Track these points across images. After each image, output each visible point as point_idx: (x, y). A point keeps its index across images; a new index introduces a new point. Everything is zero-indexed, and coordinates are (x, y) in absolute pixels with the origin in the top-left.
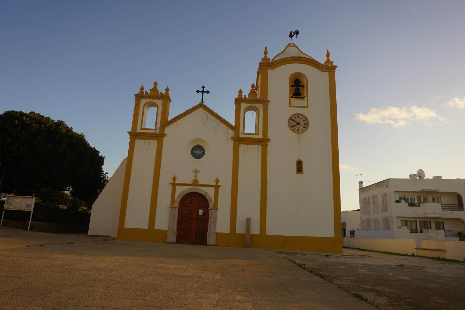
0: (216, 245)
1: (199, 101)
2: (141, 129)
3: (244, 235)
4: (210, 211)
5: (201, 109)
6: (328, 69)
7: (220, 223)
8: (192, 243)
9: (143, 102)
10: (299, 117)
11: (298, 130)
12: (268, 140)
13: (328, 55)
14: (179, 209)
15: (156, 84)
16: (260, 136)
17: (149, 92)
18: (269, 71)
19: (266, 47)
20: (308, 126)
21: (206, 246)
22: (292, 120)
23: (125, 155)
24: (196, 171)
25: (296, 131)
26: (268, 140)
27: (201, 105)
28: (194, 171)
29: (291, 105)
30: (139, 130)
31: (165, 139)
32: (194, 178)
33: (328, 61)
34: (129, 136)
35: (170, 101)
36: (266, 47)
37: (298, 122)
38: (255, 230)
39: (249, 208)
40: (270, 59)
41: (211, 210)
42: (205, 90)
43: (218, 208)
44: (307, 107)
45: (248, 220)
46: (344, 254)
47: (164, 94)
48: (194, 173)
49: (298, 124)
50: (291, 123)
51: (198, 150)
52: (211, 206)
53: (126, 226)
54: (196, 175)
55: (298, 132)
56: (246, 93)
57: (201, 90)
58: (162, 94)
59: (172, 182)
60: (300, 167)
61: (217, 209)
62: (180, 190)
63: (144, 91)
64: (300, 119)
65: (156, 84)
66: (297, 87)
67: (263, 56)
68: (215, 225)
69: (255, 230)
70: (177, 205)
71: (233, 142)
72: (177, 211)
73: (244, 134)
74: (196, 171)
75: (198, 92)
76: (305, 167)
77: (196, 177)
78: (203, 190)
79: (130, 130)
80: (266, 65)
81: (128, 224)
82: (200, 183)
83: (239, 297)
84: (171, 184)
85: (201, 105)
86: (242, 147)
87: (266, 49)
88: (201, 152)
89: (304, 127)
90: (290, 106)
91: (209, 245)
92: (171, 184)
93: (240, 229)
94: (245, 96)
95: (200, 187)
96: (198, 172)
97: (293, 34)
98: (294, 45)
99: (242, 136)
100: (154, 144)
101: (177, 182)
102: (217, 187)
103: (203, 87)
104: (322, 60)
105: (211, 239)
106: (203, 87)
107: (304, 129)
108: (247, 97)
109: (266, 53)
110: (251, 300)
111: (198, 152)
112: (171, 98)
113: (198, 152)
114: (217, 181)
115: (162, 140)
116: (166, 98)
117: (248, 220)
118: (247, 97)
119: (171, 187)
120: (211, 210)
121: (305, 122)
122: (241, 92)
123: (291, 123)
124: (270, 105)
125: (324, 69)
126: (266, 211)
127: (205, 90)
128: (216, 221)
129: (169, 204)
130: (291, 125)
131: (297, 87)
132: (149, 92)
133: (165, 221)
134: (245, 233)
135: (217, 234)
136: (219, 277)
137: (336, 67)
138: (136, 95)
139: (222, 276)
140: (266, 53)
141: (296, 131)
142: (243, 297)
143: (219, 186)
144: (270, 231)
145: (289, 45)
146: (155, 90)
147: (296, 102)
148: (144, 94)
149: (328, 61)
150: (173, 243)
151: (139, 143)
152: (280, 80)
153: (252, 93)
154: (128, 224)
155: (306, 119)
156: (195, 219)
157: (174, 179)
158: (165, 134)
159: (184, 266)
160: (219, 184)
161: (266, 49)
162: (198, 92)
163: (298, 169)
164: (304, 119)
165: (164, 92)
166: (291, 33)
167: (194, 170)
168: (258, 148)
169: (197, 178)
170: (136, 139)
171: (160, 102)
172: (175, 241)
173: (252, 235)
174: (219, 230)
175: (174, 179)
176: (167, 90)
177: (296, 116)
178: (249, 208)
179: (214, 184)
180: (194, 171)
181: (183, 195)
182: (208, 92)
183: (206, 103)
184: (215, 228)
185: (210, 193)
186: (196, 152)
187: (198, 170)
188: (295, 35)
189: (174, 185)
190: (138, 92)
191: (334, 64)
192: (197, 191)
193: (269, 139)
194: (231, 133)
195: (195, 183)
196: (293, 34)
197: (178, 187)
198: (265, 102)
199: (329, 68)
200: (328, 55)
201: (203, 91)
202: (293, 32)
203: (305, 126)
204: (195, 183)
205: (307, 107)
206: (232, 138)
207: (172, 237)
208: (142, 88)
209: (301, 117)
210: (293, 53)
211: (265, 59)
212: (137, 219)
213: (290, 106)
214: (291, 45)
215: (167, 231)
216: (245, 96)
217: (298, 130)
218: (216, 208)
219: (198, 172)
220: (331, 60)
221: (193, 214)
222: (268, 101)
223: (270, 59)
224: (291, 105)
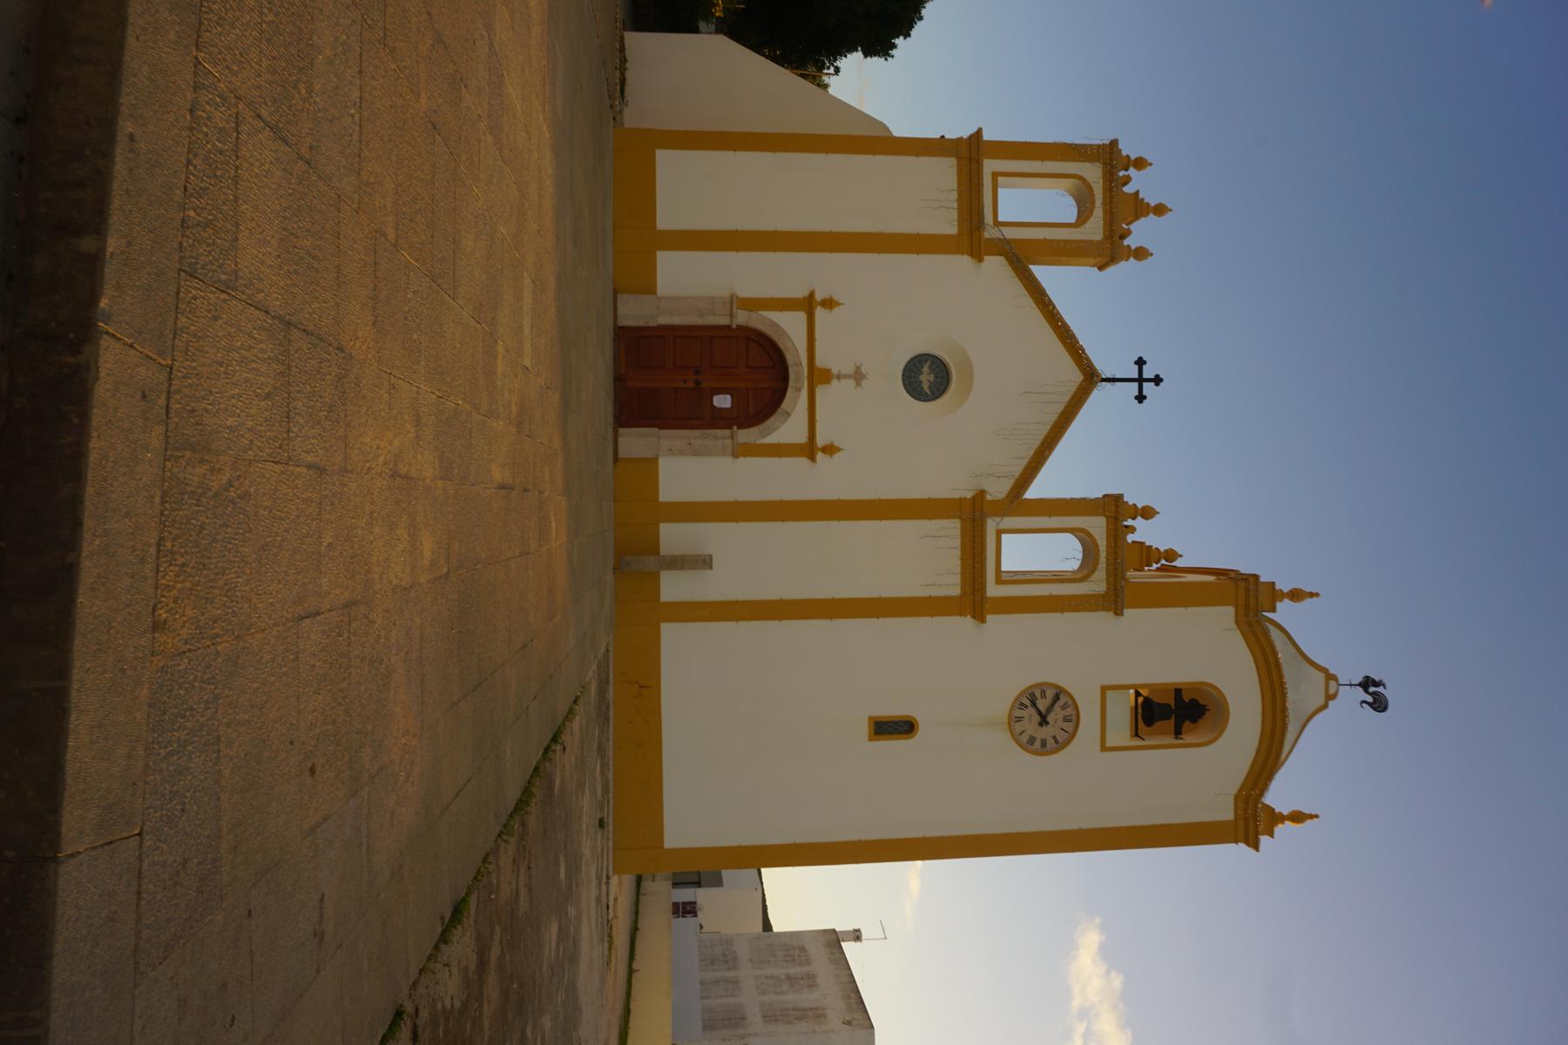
0: (616, 459)
1: (1105, 369)
2: (995, 175)
3: (655, 550)
4: (727, 432)
5: (1079, 377)
6: (1246, 819)
7: (689, 469)
8: (619, 380)
9: (1093, 172)
10: (1066, 719)
11: (1019, 719)
13: (1298, 817)
14: (729, 327)
15: (1160, 210)
16: (993, 590)
17: (1128, 189)
18: (1230, 610)
20: (1036, 753)
21: (610, 430)
22: (1057, 698)
23: (899, 131)
24: (858, 376)
25: (1018, 713)
27: (1091, 378)
28: (858, 368)
29: (1109, 694)
30: (990, 166)
31: (965, 261)
32: (835, 371)
33: (1275, 818)
34: (966, 135)
35: (1101, 268)
37: (1049, 719)
38: (674, 587)
39: (744, 561)
40: (1274, 611)
41: (732, 437)
42: (1148, 388)
43: (741, 459)
44: (1104, 748)
45: (705, 562)
46: (614, 880)
47: (1126, 242)
48: (851, 371)
49: (1044, 716)
50: (1043, 692)
52: (745, 435)
54: (847, 377)
55: (1014, 720)
56: (1143, 532)
57: (1148, 373)
58: (1123, 237)
59: (819, 297)
61: (735, 455)
62: (790, 327)
63: (1132, 171)
64: (1061, 723)
65: (1160, 210)
66: (1175, 712)
67: (1284, 586)
68: (681, 453)
69: (674, 587)
70: (742, 318)
71: (969, 495)
72: (723, 321)
73: (999, 533)
74: (858, 376)
75: (1140, 362)
77: (839, 377)
79: (987, 136)
80: (1248, 598)
81: (667, 162)
82: (820, 392)
83: (427, 545)
84: (812, 294)
85: (1091, 378)
86: (951, 529)
87: (1312, 595)
88: (926, 387)
89: (1032, 740)
90: (1104, 689)
92: (812, 294)
93: (674, 537)
94: (1132, 529)
96: (858, 384)
97: (1372, 689)
98: (1330, 697)
99: (991, 525)
100: (946, 223)
101: (819, 312)
102: (809, 450)
103: (1157, 380)
104: (1277, 797)
105: (635, 442)
106: (1157, 380)
107: (1024, 738)
108: (1130, 538)
109: (1296, 595)
110: (422, 580)
111: (928, 377)
112: (1111, 270)
113: (926, 378)
114: (830, 450)
115: (959, 252)
116: (1110, 250)
117: (705, 562)
118: (1130, 538)
119: (801, 293)
120: (732, 437)
121: (1051, 743)
122: (1148, 513)
123: (1043, 692)
124: (1104, 618)
125: (1246, 803)
126: (738, 619)
127: (1148, 388)
128: (696, 453)
129: (743, 293)
130: (1038, 695)
131: (1175, 712)
132: (1128, 189)
133: (687, 284)
134: (663, 552)
135: (655, 461)
136: (498, 475)
137: (1257, 848)
138: (1114, 143)
139: (502, 487)
140: (1296, 595)
141: (1018, 713)
142: (428, 554)
143: (812, 458)
144: (673, 636)
145: (1330, 677)
146: (1140, 208)
147: (1122, 710)
148: (1122, 173)
149: (1275, 818)
150: (615, 315)
151: (945, 172)
152: (1200, 649)
153: (1146, 554)
154: (667, 162)
155: (1060, 745)
156: (698, 383)
157: (829, 304)
158: (980, 260)
159: (524, 351)
160: (820, 456)
161: (1312, 595)
162: (1140, 362)
163: (885, 723)
164: (1061, 737)
165: (1132, 242)
166: (1377, 684)
168: (951, 585)
169: (835, 382)
170: (959, 159)
171: (1094, 230)
172: (623, 322)
173: (658, 574)
174: (665, 464)
175: (829, 304)
176: (1141, 254)
177: (1069, 711)
178: (744, 561)
179: (820, 441)
180: (858, 368)
181: (775, 338)
182: (1141, 398)
183: (1100, 393)
184: (671, 452)
185: (789, 427)
186: (926, 369)
187: (864, 383)
188: (1370, 699)
189: (808, 305)
190: (1128, 149)
191: (1264, 839)
192: (791, 383)
193: (983, 620)
194: (998, 490)
195: (819, 376)
196: (1372, 689)
197: (800, 318)
198: (1115, 600)
199: (1250, 821)
200: (1298, 817)
201: (1142, 380)
202: (1380, 689)
203: (1038, 744)
204: (819, 376)
205: (1104, 748)
206: (982, 493)
207: (634, 312)
208: (1140, 163)
209: (1069, 727)
210: (1301, 691)
211: (1273, 594)
212: (687, 189)
213: (1104, 689)
214: (1332, 683)
215: (652, 290)
216: (1132, 529)
217: (1019, 719)
218: (741, 451)
219: (858, 384)
220: (1280, 829)
221: (716, 376)
222: (1118, 612)
223: (1274, 611)
224: (1109, 694)
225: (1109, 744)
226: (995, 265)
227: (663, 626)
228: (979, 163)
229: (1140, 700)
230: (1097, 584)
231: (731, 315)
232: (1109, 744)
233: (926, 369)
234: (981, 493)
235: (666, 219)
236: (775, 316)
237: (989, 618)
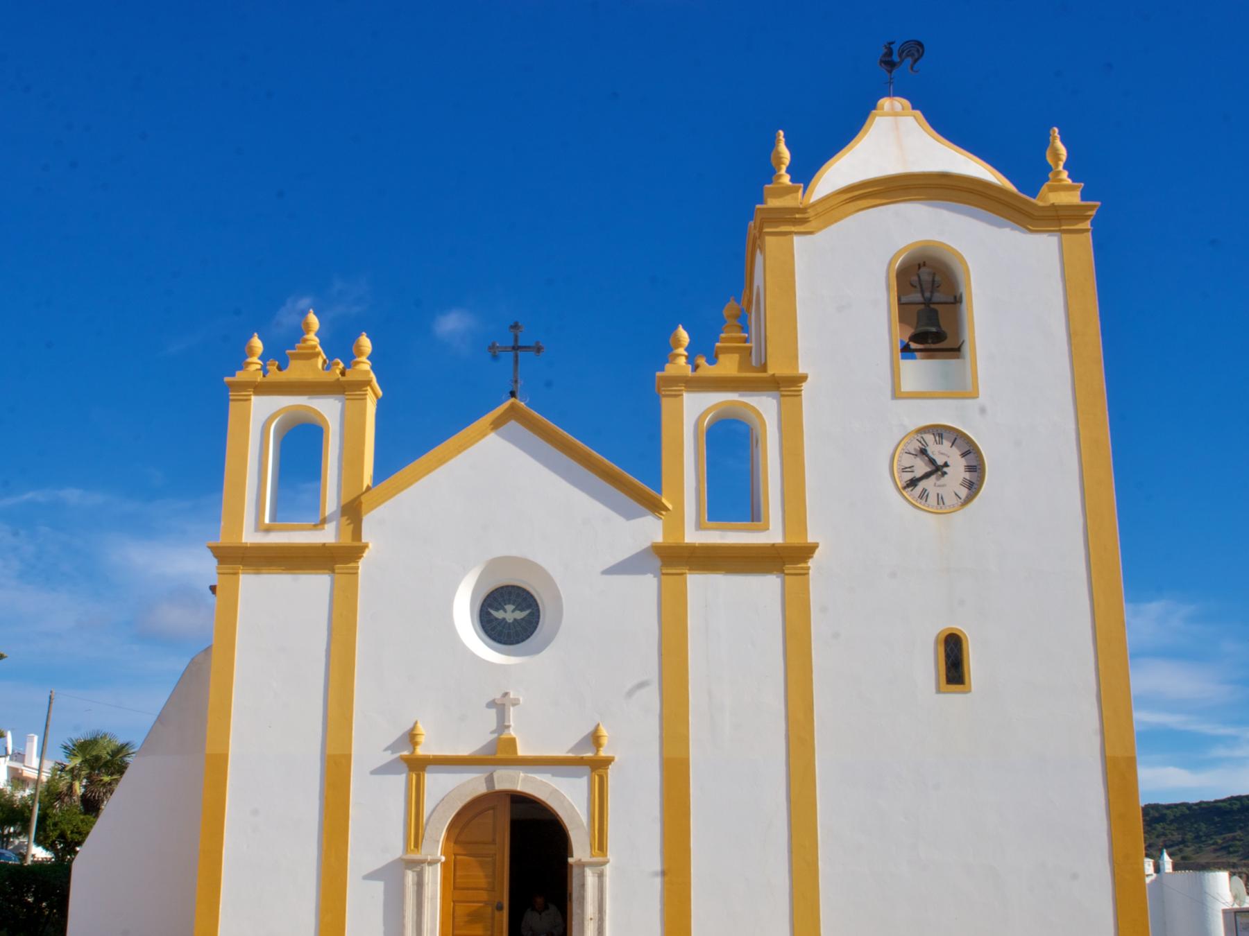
11: (940, 499)
12: (805, 552)
16: (772, 535)
19: (609, 571)
25: (932, 500)
36: (609, 571)
50: (904, 470)
51: (510, 607)
60: (953, 661)
77: (502, 726)
82: (522, 752)
86: (698, 584)
88: (520, 615)
99: (693, 536)
114: (595, 739)
130: (908, 476)
141: (932, 500)
143: (607, 762)
157: (411, 737)
160: (603, 753)
167: (498, 696)
168: (765, 588)
169: (512, 733)
186: (499, 615)
217: (940, 499)
229: (913, 345)
233: (499, 615)
236: (427, 807)
237: (811, 539)
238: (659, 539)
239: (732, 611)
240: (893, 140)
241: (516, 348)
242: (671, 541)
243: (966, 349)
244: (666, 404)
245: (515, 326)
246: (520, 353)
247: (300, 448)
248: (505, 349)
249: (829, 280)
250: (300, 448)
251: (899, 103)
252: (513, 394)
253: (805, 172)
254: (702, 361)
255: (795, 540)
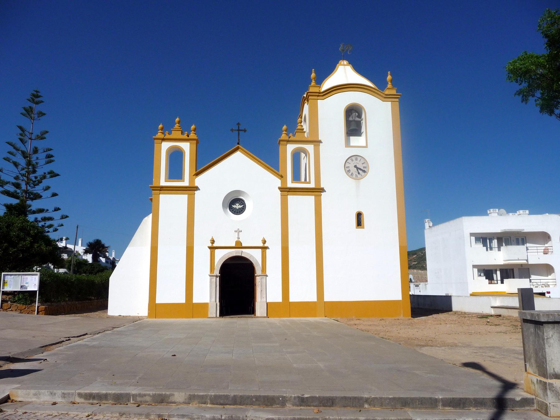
10: (357, 159)
16: (312, 185)
18: (319, 102)
24: (239, 231)
25: (354, 176)
26: (322, 190)
32: (236, 239)
43: (267, 273)
44: (366, 147)
52: (258, 271)
53: (159, 301)
59: (210, 245)
60: (359, 220)
62: (221, 256)
64: (358, 161)
70: (217, 272)
72: (218, 279)
74: (239, 231)
76: (366, 220)
78: (246, 253)
82: (243, 245)
84: (210, 248)
86: (292, 199)
91: (258, 317)
92: (210, 248)
95: (244, 250)
99: (290, 184)
100: (183, 198)
101: (215, 245)
102: (264, 248)
114: (264, 242)
119: (209, 250)
125: (385, 98)
133: (206, 291)
143: (267, 248)
144: (328, 297)
147: (354, 140)
157: (213, 242)
160: (266, 245)
164: (362, 161)
168: (310, 199)
169: (240, 240)
175: (213, 242)
179: (261, 245)
185: (255, 256)
189: (212, 248)
195: (239, 246)
197: (217, 251)
204: (239, 246)
205: (366, 147)
209: (359, 158)
212: (171, 293)
225: (365, 145)
226: (199, 181)
227: (325, 300)
228: (162, 187)
230: (310, 148)
231: (217, 276)
232: (365, 145)
234: (279, 188)
235: (183, 300)
238: (280, 186)
239: (301, 205)
240: (344, 73)
241: (239, 130)
242: (284, 187)
243: (364, 135)
244: (281, 147)
245: (238, 124)
246: (240, 132)
247: (176, 157)
248: (236, 130)
249: (328, 113)
250: (176, 157)
251: (345, 62)
252: (238, 144)
253: (320, 81)
254: (291, 135)
255: (318, 187)
